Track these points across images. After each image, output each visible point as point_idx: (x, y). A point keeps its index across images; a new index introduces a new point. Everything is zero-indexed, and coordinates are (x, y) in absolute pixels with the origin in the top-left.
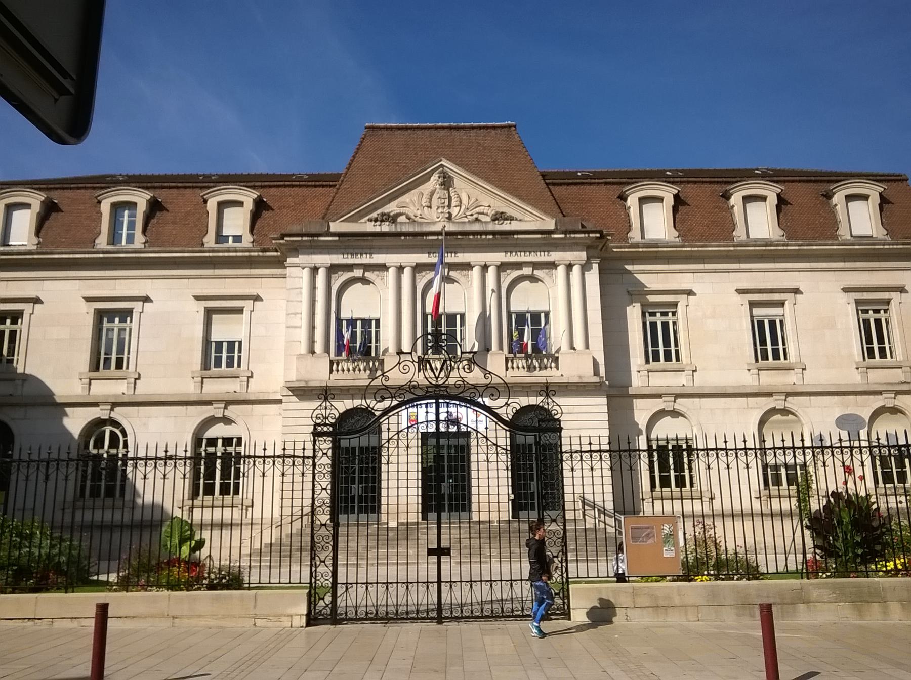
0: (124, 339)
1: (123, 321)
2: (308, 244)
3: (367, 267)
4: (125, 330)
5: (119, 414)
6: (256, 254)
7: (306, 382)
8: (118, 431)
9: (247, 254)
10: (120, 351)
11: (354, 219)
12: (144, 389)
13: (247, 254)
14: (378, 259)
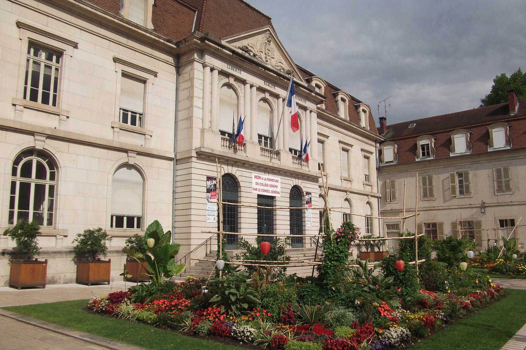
0: (50, 77)
1: (49, 58)
2: (213, 50)
3: (237, 79)
4: (50, 68)
5: (52, 147)
6: (163, 41)
7: (212, 150)
8: (44, 163)
9: (157, 39)
10: (46, 86)
11: (229, 42)
12: (72, 127)
13: (157, 39)
14: (244, 75)
